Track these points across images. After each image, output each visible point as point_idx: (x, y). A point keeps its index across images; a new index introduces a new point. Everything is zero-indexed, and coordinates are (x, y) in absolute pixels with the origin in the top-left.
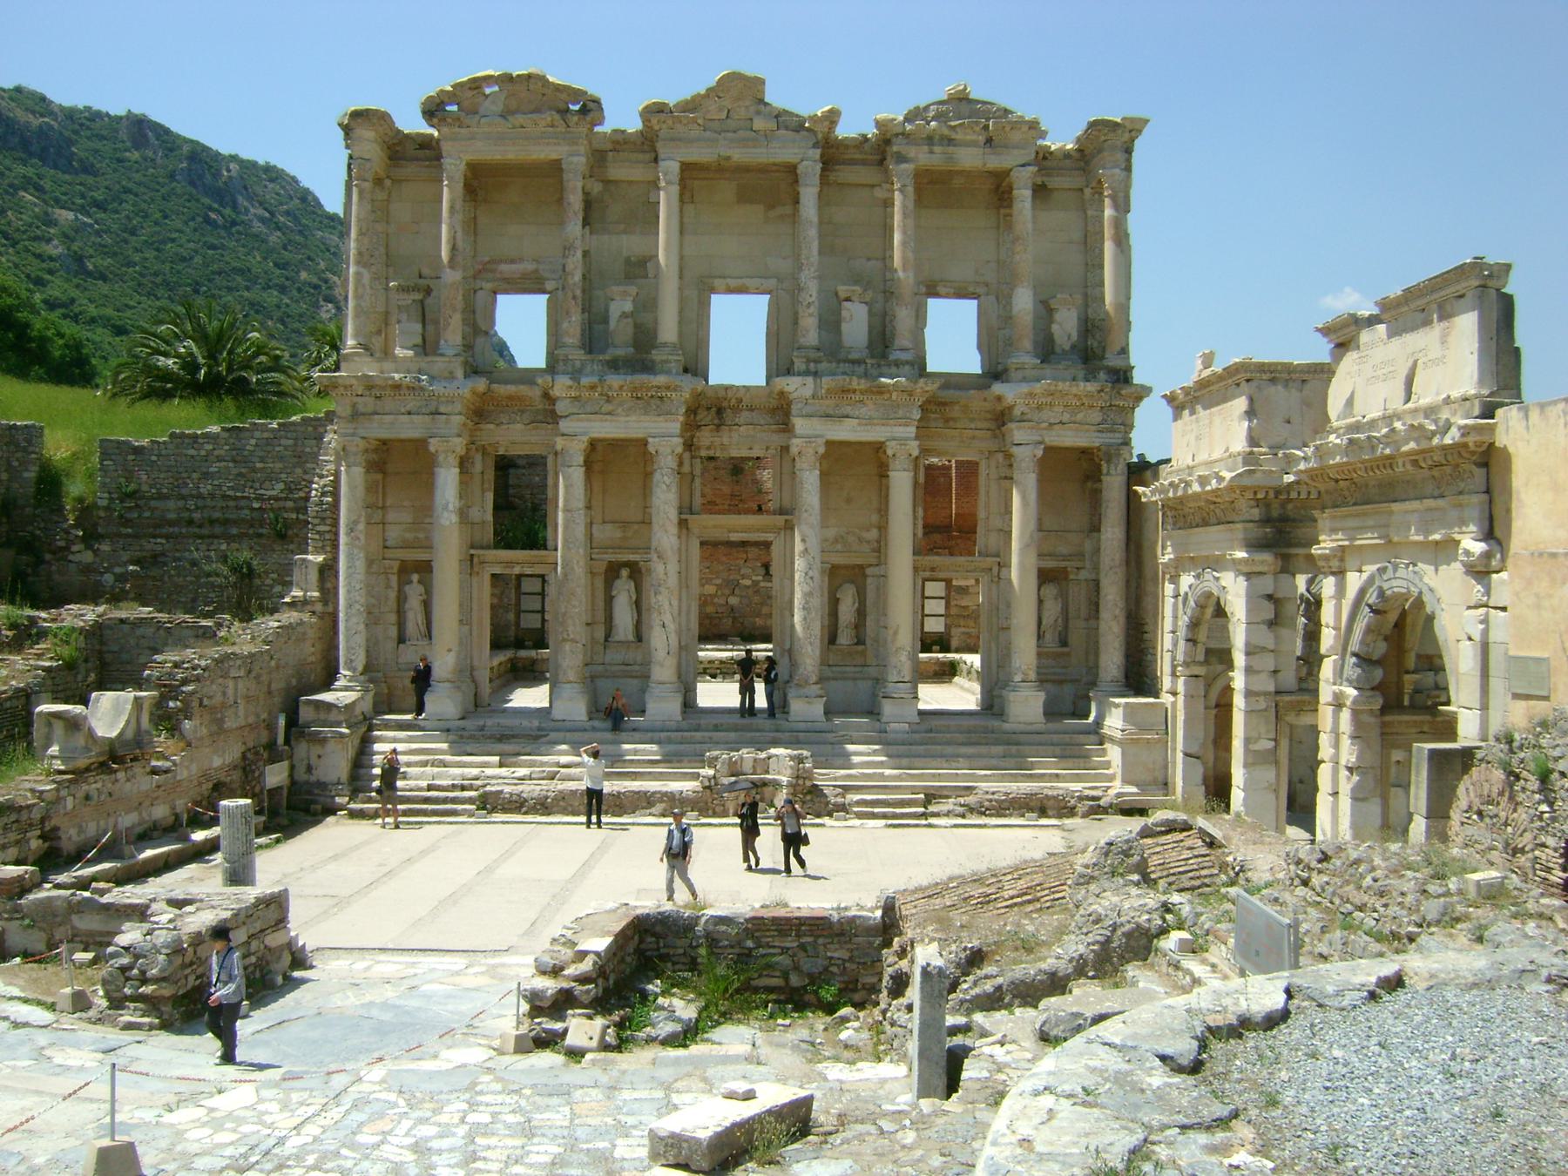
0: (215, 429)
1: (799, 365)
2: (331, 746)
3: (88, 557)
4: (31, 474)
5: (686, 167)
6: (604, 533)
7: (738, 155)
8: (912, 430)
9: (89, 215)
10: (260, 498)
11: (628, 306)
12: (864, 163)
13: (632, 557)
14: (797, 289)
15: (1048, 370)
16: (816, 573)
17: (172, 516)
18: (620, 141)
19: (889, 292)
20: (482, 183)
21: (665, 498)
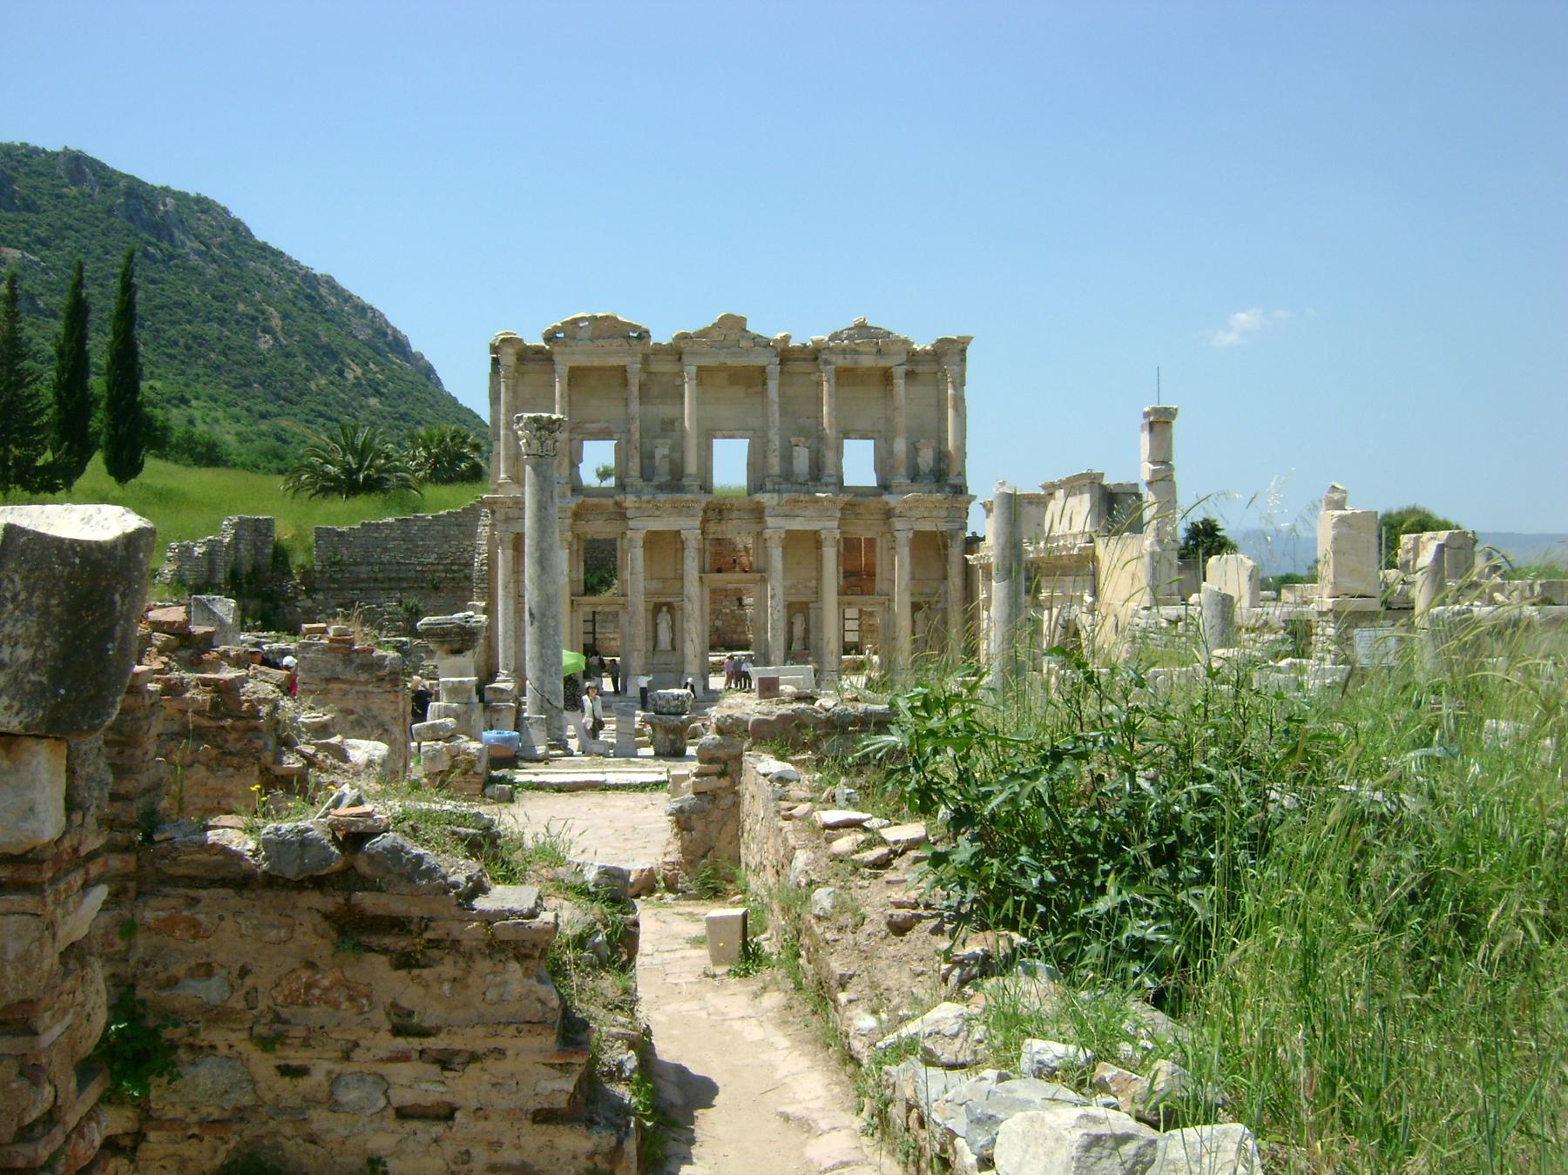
0: (390, 520)
1: (769, 486)
2: (504, 713)
3: (309, 603)
4: (269, 550)
5: (700, 369)
6: (656, 585)
7: (730, 362)
8: (835, 524)
9: (35, 254)
10: (421, 564)
11: (666, 451)
12: (804, 360)
13: (669, 600)
14: (766, 441)
15: (915, 486)
16: (780, 607)
17: (363, 576)
18: (659, 350)
19: (821, 438)
20: (576, 376)
21: (692, 566)
